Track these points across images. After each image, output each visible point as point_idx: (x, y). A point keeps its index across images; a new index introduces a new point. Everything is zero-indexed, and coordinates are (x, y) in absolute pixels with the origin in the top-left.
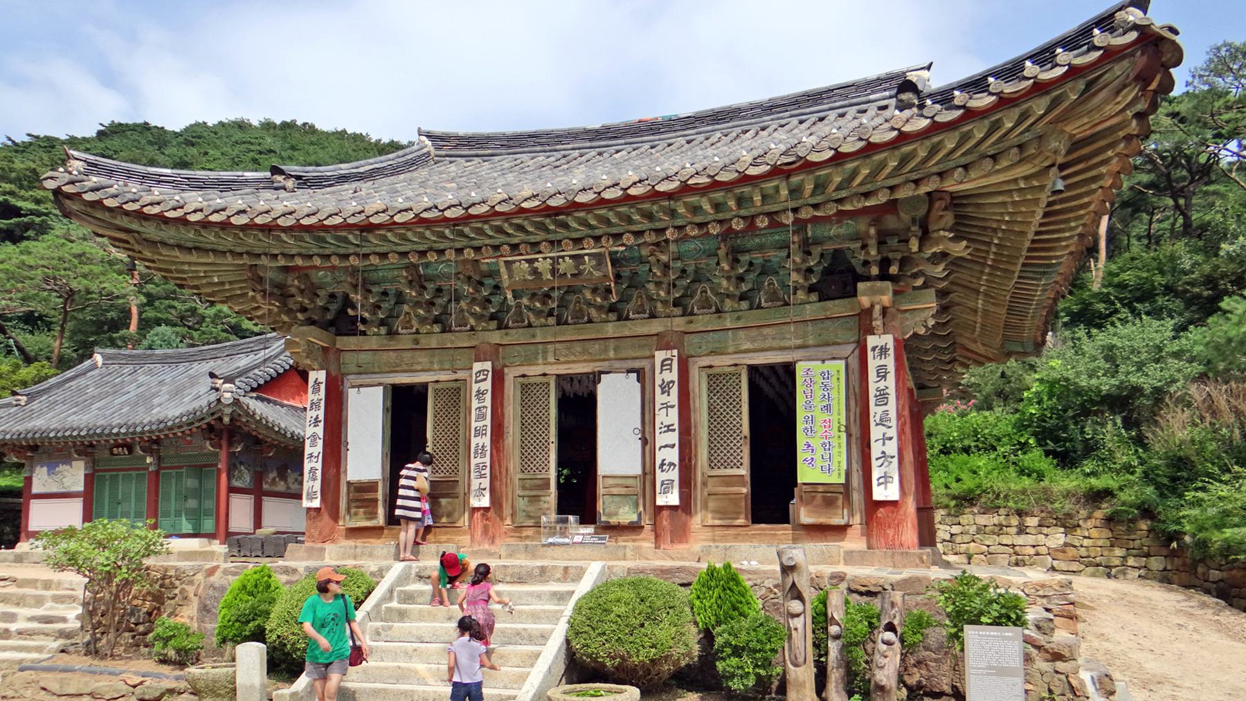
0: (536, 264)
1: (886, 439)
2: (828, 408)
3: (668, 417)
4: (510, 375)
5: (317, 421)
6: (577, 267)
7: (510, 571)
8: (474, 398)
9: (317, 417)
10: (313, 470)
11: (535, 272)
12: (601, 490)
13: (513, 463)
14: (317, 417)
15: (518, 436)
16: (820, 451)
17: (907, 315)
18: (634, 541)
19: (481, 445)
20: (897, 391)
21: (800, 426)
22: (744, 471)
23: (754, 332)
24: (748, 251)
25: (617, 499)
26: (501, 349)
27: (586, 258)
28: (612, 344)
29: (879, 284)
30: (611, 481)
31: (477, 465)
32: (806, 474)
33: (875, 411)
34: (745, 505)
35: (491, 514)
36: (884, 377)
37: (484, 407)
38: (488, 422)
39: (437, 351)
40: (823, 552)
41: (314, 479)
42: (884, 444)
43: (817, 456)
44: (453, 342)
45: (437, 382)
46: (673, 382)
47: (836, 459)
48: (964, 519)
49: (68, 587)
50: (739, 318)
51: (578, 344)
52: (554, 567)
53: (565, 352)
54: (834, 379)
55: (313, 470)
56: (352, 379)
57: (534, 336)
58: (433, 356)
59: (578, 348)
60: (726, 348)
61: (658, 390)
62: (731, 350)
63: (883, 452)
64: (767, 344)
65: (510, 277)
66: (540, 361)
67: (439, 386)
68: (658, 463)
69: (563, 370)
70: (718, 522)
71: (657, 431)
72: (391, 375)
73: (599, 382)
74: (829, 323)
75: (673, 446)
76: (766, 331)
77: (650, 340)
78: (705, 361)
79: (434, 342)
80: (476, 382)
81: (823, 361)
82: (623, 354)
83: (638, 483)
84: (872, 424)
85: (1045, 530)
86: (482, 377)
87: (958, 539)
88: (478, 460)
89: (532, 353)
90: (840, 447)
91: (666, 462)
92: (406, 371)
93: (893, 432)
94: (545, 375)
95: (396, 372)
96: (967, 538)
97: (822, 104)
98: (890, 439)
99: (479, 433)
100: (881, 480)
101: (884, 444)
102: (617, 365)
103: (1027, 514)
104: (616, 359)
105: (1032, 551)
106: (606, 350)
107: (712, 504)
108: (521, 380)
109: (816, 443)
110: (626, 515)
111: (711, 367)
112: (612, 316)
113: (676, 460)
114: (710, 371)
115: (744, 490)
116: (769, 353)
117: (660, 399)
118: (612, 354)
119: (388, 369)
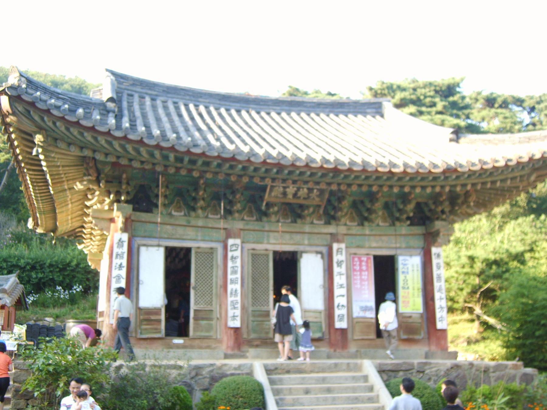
0: (288, 190)
1: (441, 299)
5: (121, 266)
6: (308, 194)
11: (285, 194)
15: (250, 285)
19: (234, 290)
23: (377, 238)
26: (242, 232)
27: (315, 191)
28: (306, 236)
31: (232, 302)
37: (236, 267)
38: (239, 275)
45: (198, 248)
46: (342, 261)
50: (372, 230)
52: (342, 363)
57: (263, 227)
59: (287, 236)
61: (335, 265)
64: (384, 245)
66: (266, 241)
67: (199, 250)
68: (336, 304)
69: (279, 248)
73: (301, 257)
75: (343, 296)
76: (384, 238)
80: (231, 251)
83: (323, 315)
86: (234, 248)
88: (233, 298)
91: (341, 304)
94: (266, 250)
99: (232, 282)
102: (308, 248)
108: (251, 251)
117: (336, 269)
118: (306, 242)
119: (166, 236)
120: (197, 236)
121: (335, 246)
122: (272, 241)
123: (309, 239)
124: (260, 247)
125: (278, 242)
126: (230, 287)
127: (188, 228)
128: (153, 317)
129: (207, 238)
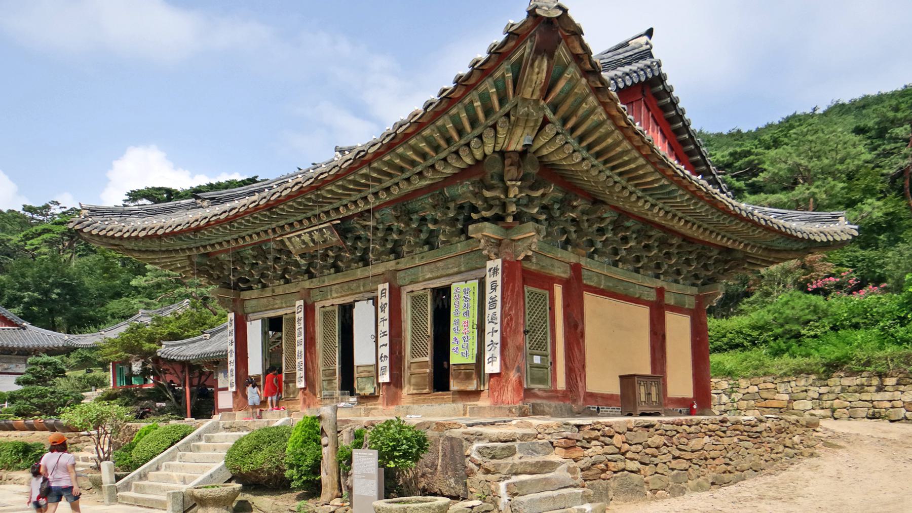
2: (467, 313)
3: (384, 327)
4: (318, 306)
12: (356, 375)
13: (320, 361)
16: (462, 343)
17: (519, 243)
18: (375, 405)
20: (503, 298)
21: (452, 326)
22: (428, 359)
23: (433, 266)
24: (417, 212)
25: (364, 380)
28: (361, 282)
29: (480, 225)
30: (361, 369)
32: (455, 358)
33: (489, 312)
34: (428, 380)
35: (307, 391)
36: (495, 289)
40: (455, 409)
42: (492, 335)
43: (460, 347)
44: (289, 289)
47: (471, 347)
48: (831, 382)
50: (422, 258)
51: (346, 284)
54: (471, 293)
55: (232, 370)
56: (251, 316)
62: (421, 279)
63: (492, 341)
65: (294, 247)
66: (329, 297)
67: (287, 317)
69: (341, 301)
70: (415, 392)
71: (379, 336)
74: (473, 254)
75: (386, 345)
76: (440, 264)
77: (380, 277)
78: (409, 288)
79: (280, 290)
81: (466, 282)
84: (487, 322)
85: (902, 388)
87: (825, 397)
89: (324, 291)
90: (473, 339)
93: (498, 327)
94: (333, 305)
95: (266, 310)
96: (832, 396)
98: (496, 331)
100: (490, 360)
101: (492, 335)
103: (886, 375)
105: (888, 405)
106: (359, 287)
107: (413, 381)
108: (322, 309)
109: (460, 337)
110: (369, 390)
111: (412, 291)
112: (361, 264)
114: (412, 294)
115: (428, 371)
116: (442, 279)
118: (362, 289)
122: (335, 295)
124: (327, 303)
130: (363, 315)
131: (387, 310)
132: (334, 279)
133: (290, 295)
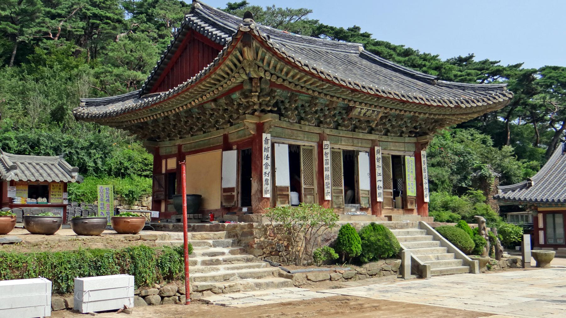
7: (399, 224)
8: (324, 156)
9: (268, 155)
10: (267, 180)
14: (268, 155)
22: (392, 191)
23: (394, 144)
28: (360, 141)
39: (306, 133)
41: (268, 184)
44: (313, 130)
45: (304, 145)
49: (177, 238)
53: (347, 141)
57: (340, 134)
58: (305, 134)
60: (388, 148)
62: (389, 149)
72: (287, 140)
74: (409, 144)
75: (381, 181)
76: (397, 144)
80: (325, 149)
82: (363, 146)
86: (326, 147)
89: (336, 139)
92: (293, 139)
94: (339, 149)
97: (338, 48)
99: (327, 170)
104: (360, 147)
106: (358, 143)
108: (332, 149)
113: (382, 186)
117: (377, 164)
118: (360, 145)
120: (304, 137)
121: (376, 148)
122: (343, 143)
123: (361, 143)
124: (336, 146)
125: (346, 144)
126: (325, 173)
127: (299, 132)
128: (285, 193)
129: (309, 140)
130: (363, 161)
131: (381, 161)
132: (346, 134)
133: (311, 134)
